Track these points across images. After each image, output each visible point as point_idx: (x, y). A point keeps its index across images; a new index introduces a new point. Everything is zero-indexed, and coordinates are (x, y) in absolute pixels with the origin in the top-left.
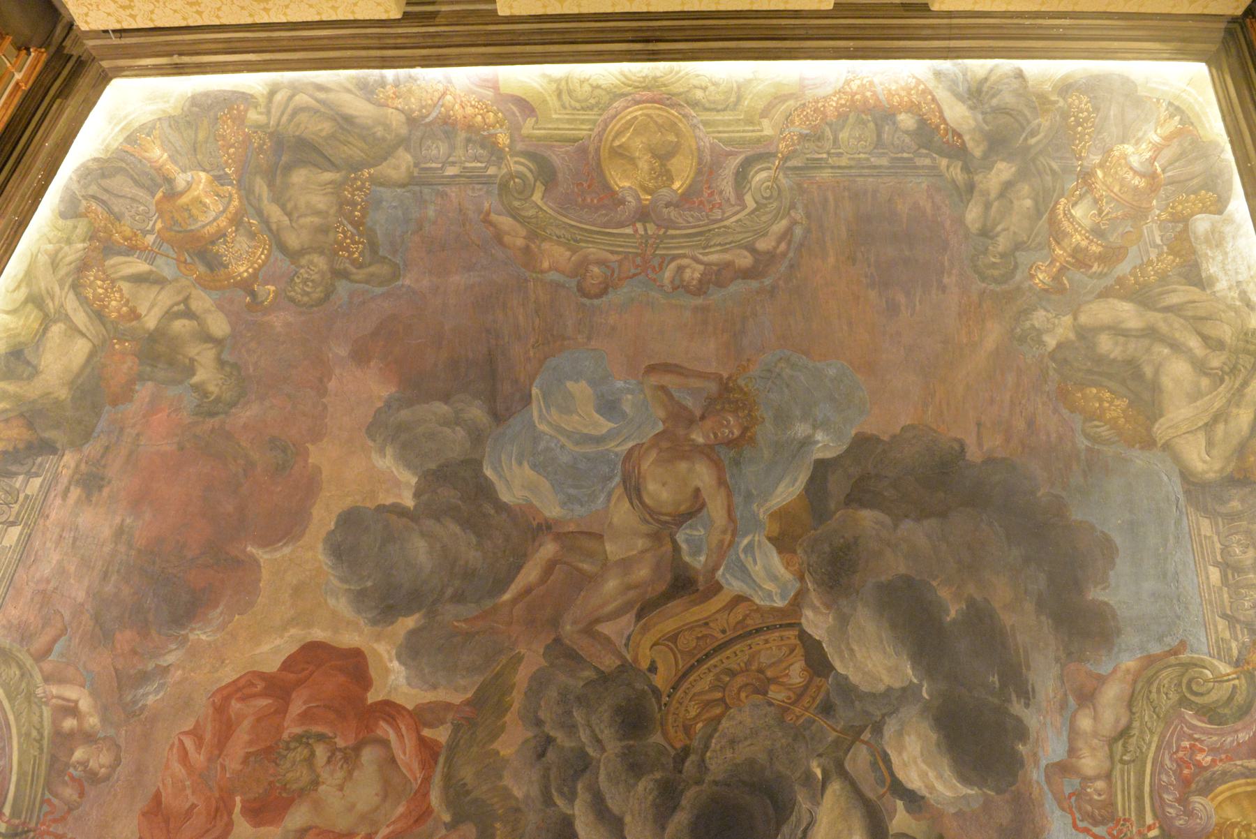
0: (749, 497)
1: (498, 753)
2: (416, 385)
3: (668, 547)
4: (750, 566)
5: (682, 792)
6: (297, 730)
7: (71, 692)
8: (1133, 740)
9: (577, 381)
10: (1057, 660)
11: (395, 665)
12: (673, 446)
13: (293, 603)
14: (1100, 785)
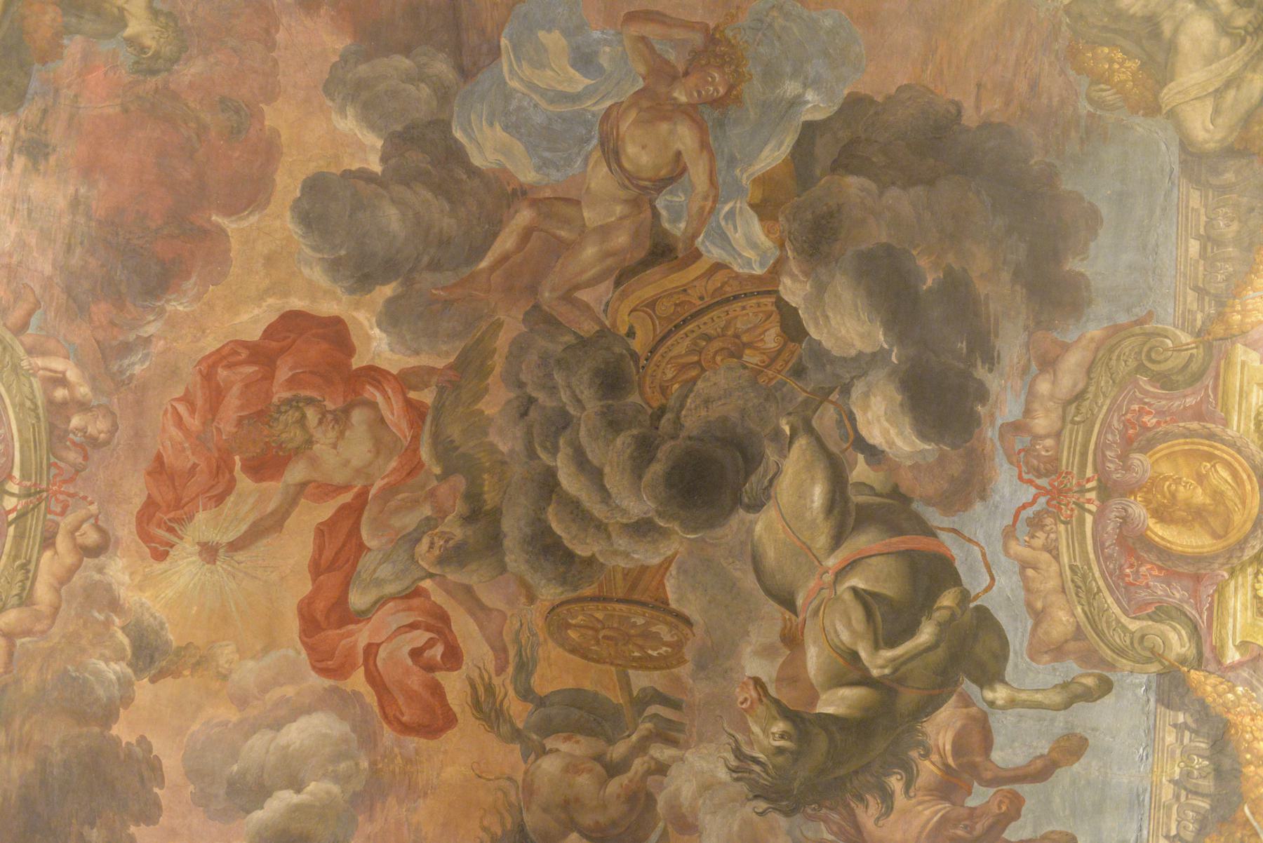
0: (732, 162)
1: (482, 412)
2: (373, 38)
3: (647, 214)
4: (730, 234)
5: (657, 448)
6: (287, 395)
7: (58, 364)
8: (1087, 403)
9: (549, 31)
10: (1026, 328)
11: (376, 332)
12: (652, 104)
13: (268, 271)
14: (1049, 442)
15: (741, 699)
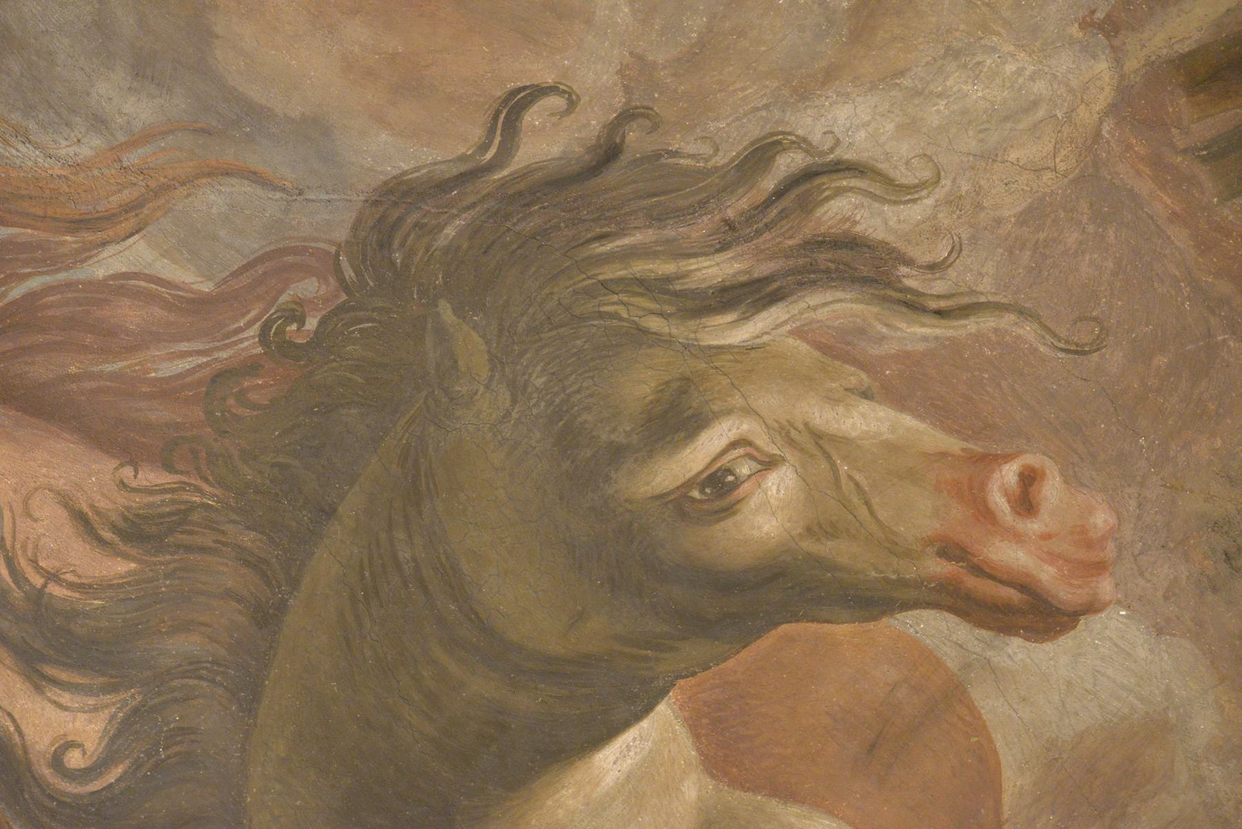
15: (1052, 490)
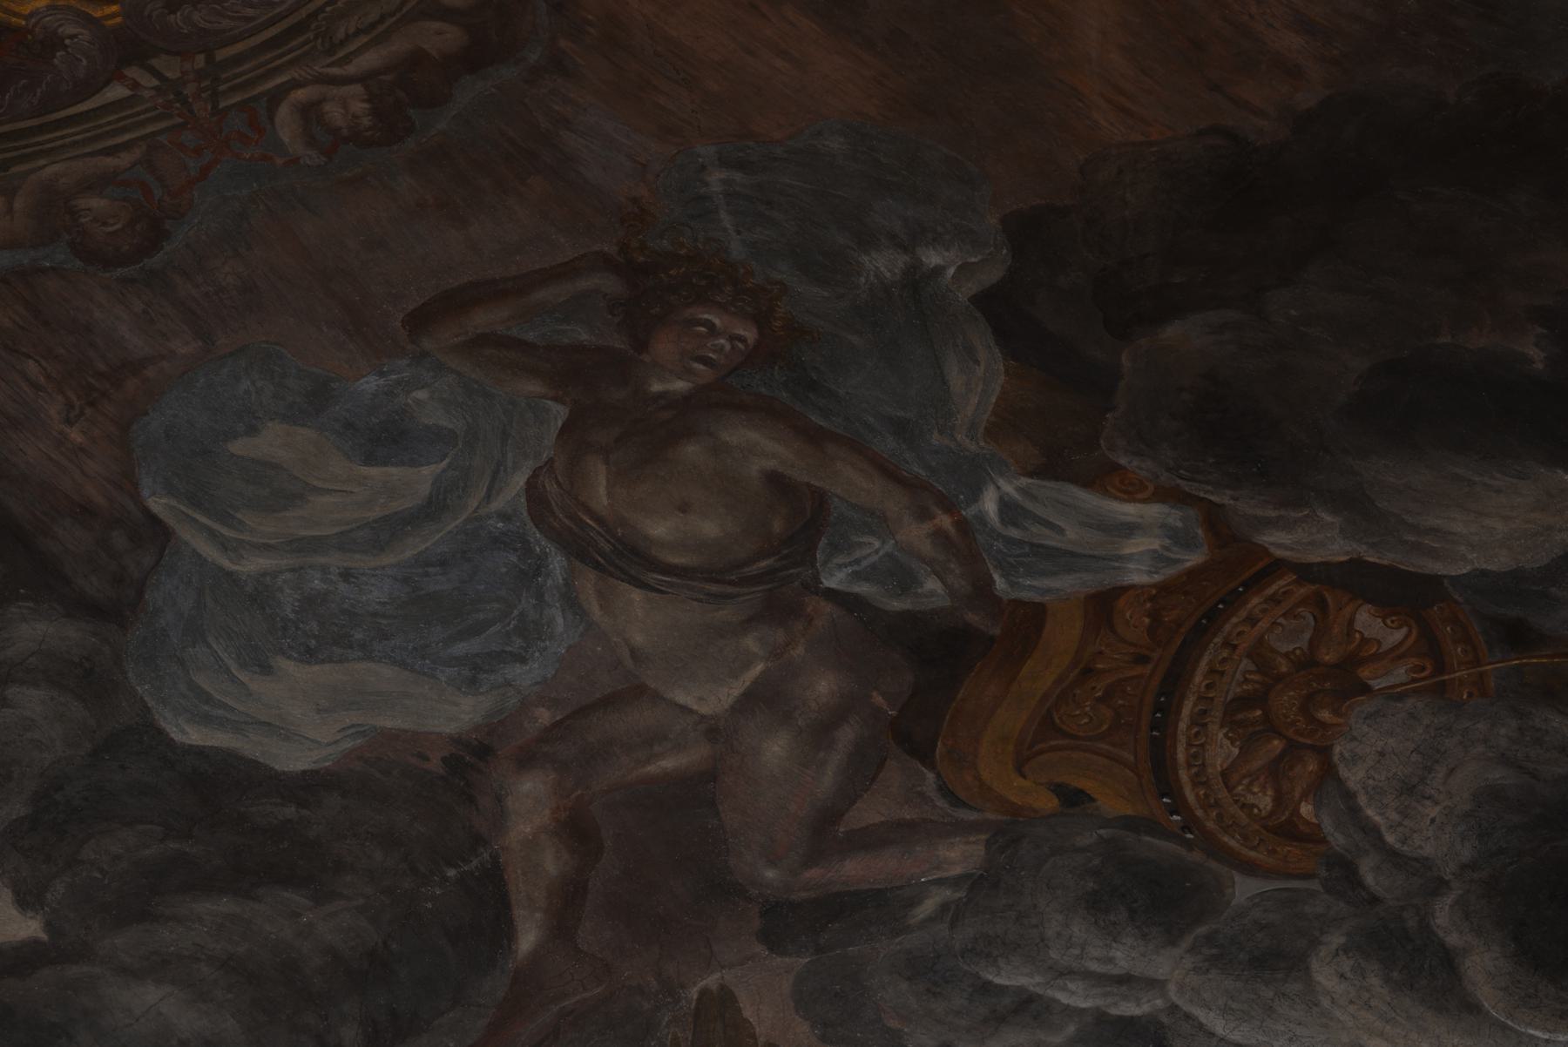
4: (1052, 540)
